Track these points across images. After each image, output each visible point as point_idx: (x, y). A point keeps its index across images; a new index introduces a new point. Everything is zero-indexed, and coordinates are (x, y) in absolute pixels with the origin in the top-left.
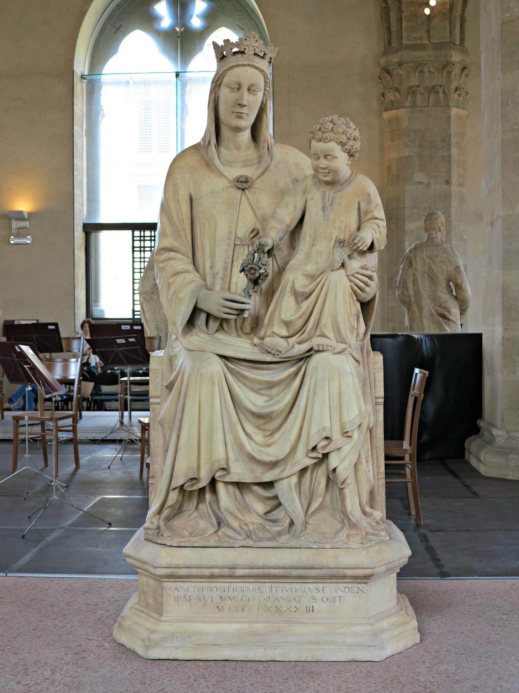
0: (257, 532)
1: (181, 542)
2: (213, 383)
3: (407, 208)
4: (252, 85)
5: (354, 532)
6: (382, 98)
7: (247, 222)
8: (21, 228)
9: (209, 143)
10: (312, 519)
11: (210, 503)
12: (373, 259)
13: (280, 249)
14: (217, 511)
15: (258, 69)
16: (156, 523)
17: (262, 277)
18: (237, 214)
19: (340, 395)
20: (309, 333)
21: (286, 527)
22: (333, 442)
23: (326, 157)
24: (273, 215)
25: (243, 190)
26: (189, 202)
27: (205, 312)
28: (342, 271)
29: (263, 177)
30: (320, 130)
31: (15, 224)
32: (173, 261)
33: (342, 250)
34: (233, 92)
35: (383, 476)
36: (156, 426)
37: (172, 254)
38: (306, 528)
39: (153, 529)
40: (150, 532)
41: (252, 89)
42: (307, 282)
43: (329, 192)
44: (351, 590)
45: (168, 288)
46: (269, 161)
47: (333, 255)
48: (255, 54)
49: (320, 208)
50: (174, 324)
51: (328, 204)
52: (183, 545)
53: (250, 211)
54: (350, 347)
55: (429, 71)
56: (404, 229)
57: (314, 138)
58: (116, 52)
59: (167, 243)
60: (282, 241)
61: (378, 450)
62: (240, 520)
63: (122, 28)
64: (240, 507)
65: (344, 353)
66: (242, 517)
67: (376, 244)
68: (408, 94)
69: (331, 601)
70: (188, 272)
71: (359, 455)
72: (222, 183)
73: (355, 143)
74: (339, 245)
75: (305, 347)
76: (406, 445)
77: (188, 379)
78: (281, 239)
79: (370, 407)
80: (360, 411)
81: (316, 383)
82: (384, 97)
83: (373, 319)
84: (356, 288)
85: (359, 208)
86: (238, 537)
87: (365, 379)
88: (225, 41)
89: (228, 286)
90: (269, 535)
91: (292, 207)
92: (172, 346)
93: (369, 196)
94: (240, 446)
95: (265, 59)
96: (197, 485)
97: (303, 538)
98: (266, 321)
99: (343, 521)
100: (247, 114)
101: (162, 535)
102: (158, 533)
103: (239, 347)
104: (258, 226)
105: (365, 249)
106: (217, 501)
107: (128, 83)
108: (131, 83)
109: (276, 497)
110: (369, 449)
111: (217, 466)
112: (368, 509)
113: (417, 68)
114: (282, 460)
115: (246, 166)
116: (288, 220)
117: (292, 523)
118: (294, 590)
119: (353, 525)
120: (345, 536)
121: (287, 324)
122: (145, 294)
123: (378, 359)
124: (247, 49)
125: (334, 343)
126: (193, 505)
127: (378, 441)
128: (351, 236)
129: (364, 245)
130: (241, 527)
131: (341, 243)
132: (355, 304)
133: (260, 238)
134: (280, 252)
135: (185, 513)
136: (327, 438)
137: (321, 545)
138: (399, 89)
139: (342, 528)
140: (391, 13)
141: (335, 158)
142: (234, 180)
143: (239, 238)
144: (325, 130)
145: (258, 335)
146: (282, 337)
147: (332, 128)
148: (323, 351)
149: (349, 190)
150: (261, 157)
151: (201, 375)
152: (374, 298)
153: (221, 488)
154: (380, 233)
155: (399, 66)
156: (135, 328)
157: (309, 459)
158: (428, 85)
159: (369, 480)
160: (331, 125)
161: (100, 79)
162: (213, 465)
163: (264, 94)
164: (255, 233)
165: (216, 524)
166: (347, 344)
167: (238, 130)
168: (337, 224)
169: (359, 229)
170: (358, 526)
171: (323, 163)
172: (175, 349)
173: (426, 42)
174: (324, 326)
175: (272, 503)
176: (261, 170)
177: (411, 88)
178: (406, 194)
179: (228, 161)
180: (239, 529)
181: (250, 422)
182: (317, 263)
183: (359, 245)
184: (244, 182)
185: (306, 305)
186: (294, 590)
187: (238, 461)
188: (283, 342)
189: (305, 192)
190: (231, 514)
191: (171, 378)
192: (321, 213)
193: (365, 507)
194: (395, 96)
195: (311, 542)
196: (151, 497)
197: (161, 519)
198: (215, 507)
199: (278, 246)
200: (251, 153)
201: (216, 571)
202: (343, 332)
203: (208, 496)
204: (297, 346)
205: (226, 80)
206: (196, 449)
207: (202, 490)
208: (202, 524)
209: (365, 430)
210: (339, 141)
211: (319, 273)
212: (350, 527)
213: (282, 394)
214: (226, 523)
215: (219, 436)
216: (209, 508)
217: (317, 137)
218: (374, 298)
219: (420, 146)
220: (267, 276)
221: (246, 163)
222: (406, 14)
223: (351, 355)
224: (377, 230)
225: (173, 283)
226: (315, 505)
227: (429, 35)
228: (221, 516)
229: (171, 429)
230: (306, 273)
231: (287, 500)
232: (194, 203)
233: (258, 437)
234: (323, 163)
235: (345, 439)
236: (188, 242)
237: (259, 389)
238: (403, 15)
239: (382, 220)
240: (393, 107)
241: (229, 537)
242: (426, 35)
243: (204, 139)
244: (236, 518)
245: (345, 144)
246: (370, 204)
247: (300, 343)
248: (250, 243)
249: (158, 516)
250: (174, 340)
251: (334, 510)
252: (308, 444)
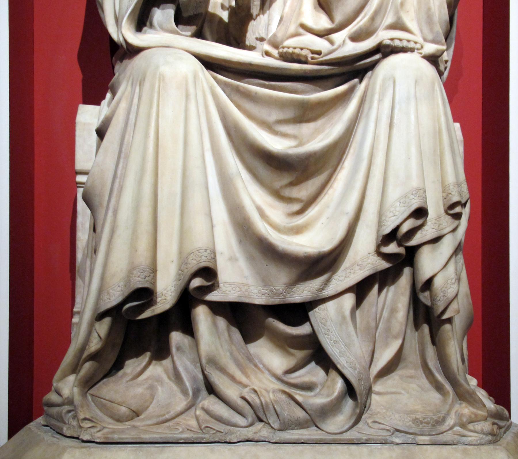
52: (116, 437)
66: (243, 379)
130: (243, 398)
153: (201, 315)
165: (191, 393)
180: (241, 403)
188: (321, 44)
204: (349, 42)
231: (335, 342)
233: (277, 212)
241: (219, 419)
244: (233, 378)
247: (355, 38)
252: (380, 224)
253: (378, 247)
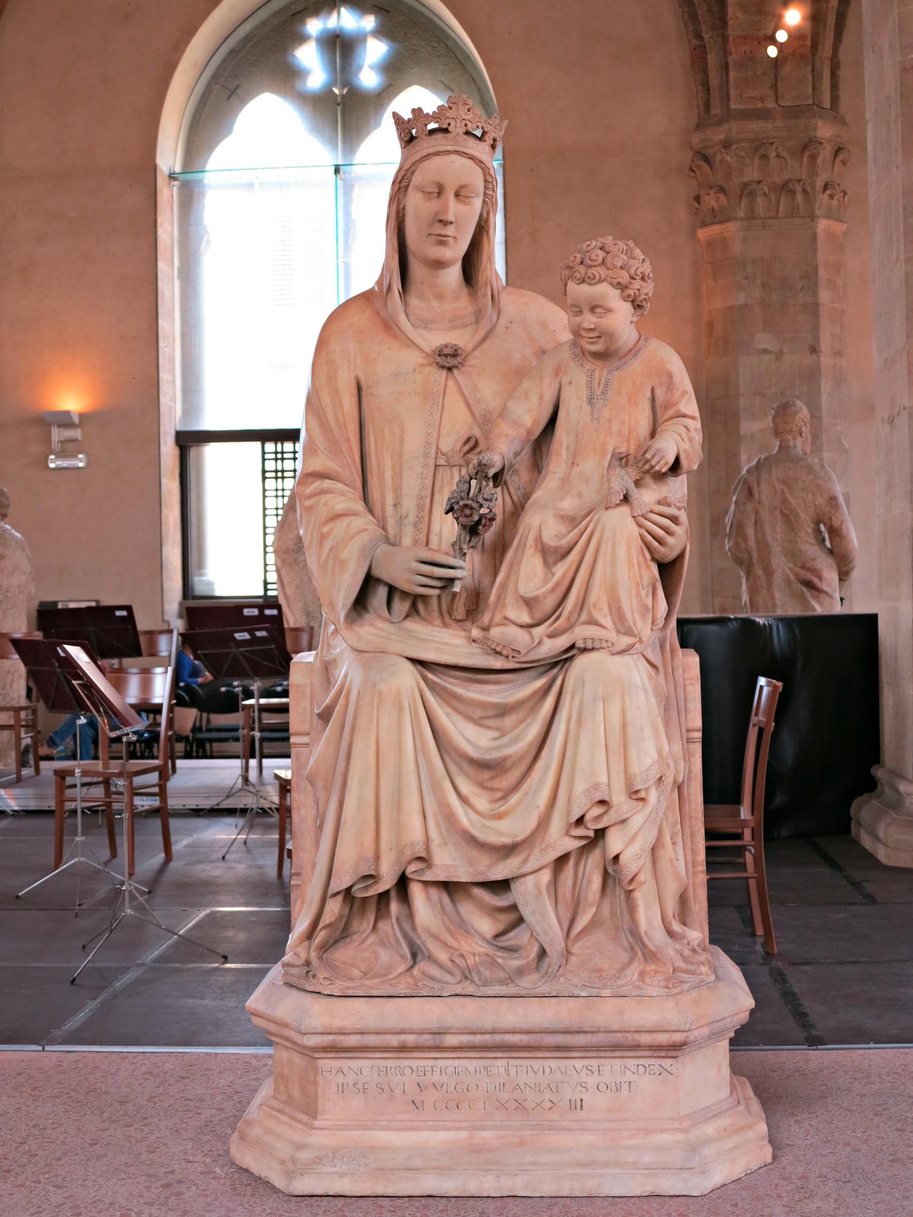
0: (482, 969)
1: (348, 988)
2: (401, 709)
4: (462, 187)
5: (653, 967)
6: (696, 204)
7: (456, 425)
9: (389, 288)
10: (578, 944)
11: (397, 919)
12: (678, 488)
13: (516, 472)
14: (410, 932)
15: (472, 158)
16: (303, 955)
17: (483, 521)
18: (439, 412)
19: (624, 726)
20: (568, 619)
21: (533, 960)
22: (613, 809)
23: (593, 309)
24: (503, 413)
25: (450, 369)
26: (355, 392)
27: (386, 584)
28: (625, 509)
29: (484, 347)
30: (582, 263)
31: (57, 434)
32: (329, 496)
33: (623, 471)
34: (430, 199)
35: (702, 867)
36: (302, 785)
37: (327, 484)
38: (567, 961)
39: (297, 966)
40: (294, 971)
41: (463, 193)
42: (563, 529)
43: (601, 371)
44: (648, 1069)
45: (321, 542)
46: (494, 319)
47: (609, 480)
48: (468, 133)
49: (585, 398)
50: (332, 605)
51: (598, 392)
52: (350, 993)
53: (462, 406)
54: (641, 641)
55: (778, 156)
56: (739, 433)
57: (571, 277)
58: (229, 132)
59: (317, 465)
60: (518, 459)
61: (693, 822)
62: (451, 947)
63: (239, 91)
64: (451, 926)
65: (630, 652)
66: (455, 944)
67: (684, 462)
68: (740, 197)
69: (614, 1089)
70: (355, 514)
71: (660, 831)
72: (412, 358)
73: (645, 285)
74: (618, 463)
75: (562, 642)
76: (745, 813)
77: (357, 701)
78: (517, 454)
79: (677, 747)
80: (660, 754)
81: (581, 706)
83: (681, 592)
84: (649, 538)
85: (653, 399)
86: (449, 978)
87: (668, 698)
88: (413, 111)
89: (425, 539)
90: (502, 975)
91: (535, 399)
92: (329, 644)
93: (670, 376)
94: (450, 819)
95: (485, 141)
96: (375, 887)
97: (562, 980)
98: (492, 598)
99: (632, 949)
100: (454, 237)
101: (314, 976)
102: (308, 972)
103: (445, 644)
104: (477, 433)
105: (664, 470)
106: (411, 916)
107: (250, 185)
108: (256, 185)
109: (514, 908)
110: (676, 822)
111: (408, 854)
112: (676, 927)
113: (757, 150)
114: (524, 842)
115: (454, 328)
116: (528, 420)
117: (543, 953)
118: (547, 1070)
119: (650, 956)
120: (636, 974)
121: (529, 603)
122: (285, 553)
123: (692, 661)
124: (453, 124)
125: (612, 635)
126: (369, 923)
127: (693, 806)
128: (639, 447)
129: (662, 462)
130: (452, 961)
131: (622, 460)
132: (648, 566)
133: (480, 453)
134: (516, 478)
135: (355, 937)
136: (602, 802)
137: (595, 992)
138: (726, 187)
139: (632, 960)
141: (610, 310)
142: (433, 351)
143: (443, 454)
144: (590, 263)
145: (480, 623)
146: (522, 626)
147: (603, 259)
148: (593, 649)
149: (635, 366)
150: (480, 312)
151: (380, 694)
152: (681, 555)
153: (416, 891)
154: (691, 440)
155: (725, 147)
156: (268, 612)
157: (572, 839)
158: (777, 180)
159: (677, 876)
160: (602, 254)
161: (202, 180)
162: (402, 852)
163: (484, 201)
164: (472, 445)
165: (409, 956)
166: (635, 636)
167: (439, 265)
168: (615, 428)
169: (653, 434)
170: (659, 956)
171: (589, 320)
172: (335, 649)
173: (771, 105)
174: (594, 605)
175: (509, 918)
176: (480, 334)
177: (745, 185)
178: (741, 371)
179: (421, 320)
180: (449, 964)
181: (467, 776)
182: (580, 495)
183: (653, 463)
184: (451, 355)
185: (562, 569)
186: (547, 1070)
187: (446, 844)
188: (521, 636)
189: (557, 372)
190: (436, 937)
191: (328, 701)
192: (586, 408)
193: (671, 923)
195: (577, 986)
196: (295, 908)
197: (312, 949)
198: (407, 927)
199: (511, 466)
200: (463, 305)
201: (410, 1039)
202: (628, 615)
203: (394, 906)
204: (546, 640)
205: (417, 179)
206: (372, 825)
207: (384, 897)
208: (385, 956)
209: (669, 787)
210: (615, 281)
211: (583, 513)
212: (645, 959)
213: (523, 726)
214: (427, 954)
215: (412, 802)
216: (396, 927)
217: (578, 275)
218: (681, 555)
219: (764, 286)
220: (492, 519)
221: (455, 323)
223: (643, 656)
224: (684, 436)
225: (329, 533)
226: (583, 921)
228: (418, 941)
229: (328, 789)
230: (562, 513)
231: (533, 912)
232: (364, 393)
233: (482, 802)
234: (589, 320)
235: (635, 803)
236: (354, 461)
237: (481, 718)
238: (730, 59)
239: (693, 418)
241: (432, 978)
242: (771, 93)
243: (380, 282)
244: (445, 944)
245: (627, 287)
246: (672, 390)
247: (552, 636)
248: (463, 462)
249: (306, 943)
250: (332, 633)
251: (617, 929)
252: (568, 813)
253: (567, 834)
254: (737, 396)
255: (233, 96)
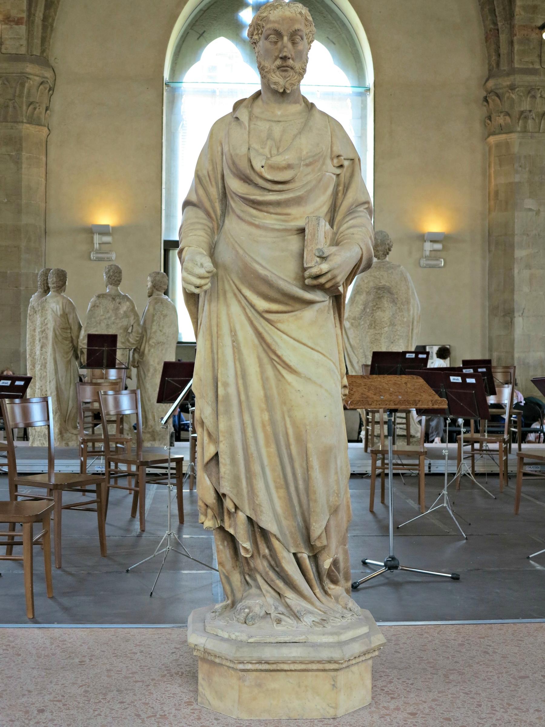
3: (517, 234)
6: (489, 122)
8: (434, 250)
31: (97, 239)
55: (541, 97)
56: (514, 257)
58: (199, 60)
63: (205, 35)
68: (519, 119)
82: (490, 120)
107: (214, 92)
108: (218, 93)
113: (529, 92)
122: (353, 319)
140: (501, 36)
155: (511, 89)
156: (421, 356)
158: (540, 110)
161: (180, 87)
173: (537, 66)
177: (522, 112)
178: (516, 220)
194: (505, 120)
219: (530, 172)
222: (518, 37)
227: (541, 60)
238: (515, 38)
240: (502, 132)
242: (537, 60)
254: (513, 235)
255: (202, 37)
